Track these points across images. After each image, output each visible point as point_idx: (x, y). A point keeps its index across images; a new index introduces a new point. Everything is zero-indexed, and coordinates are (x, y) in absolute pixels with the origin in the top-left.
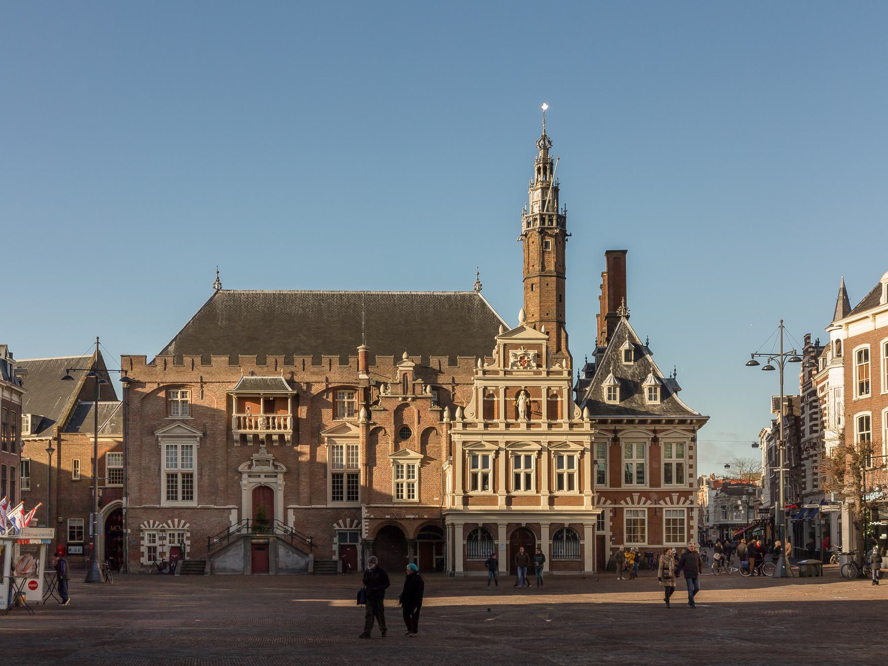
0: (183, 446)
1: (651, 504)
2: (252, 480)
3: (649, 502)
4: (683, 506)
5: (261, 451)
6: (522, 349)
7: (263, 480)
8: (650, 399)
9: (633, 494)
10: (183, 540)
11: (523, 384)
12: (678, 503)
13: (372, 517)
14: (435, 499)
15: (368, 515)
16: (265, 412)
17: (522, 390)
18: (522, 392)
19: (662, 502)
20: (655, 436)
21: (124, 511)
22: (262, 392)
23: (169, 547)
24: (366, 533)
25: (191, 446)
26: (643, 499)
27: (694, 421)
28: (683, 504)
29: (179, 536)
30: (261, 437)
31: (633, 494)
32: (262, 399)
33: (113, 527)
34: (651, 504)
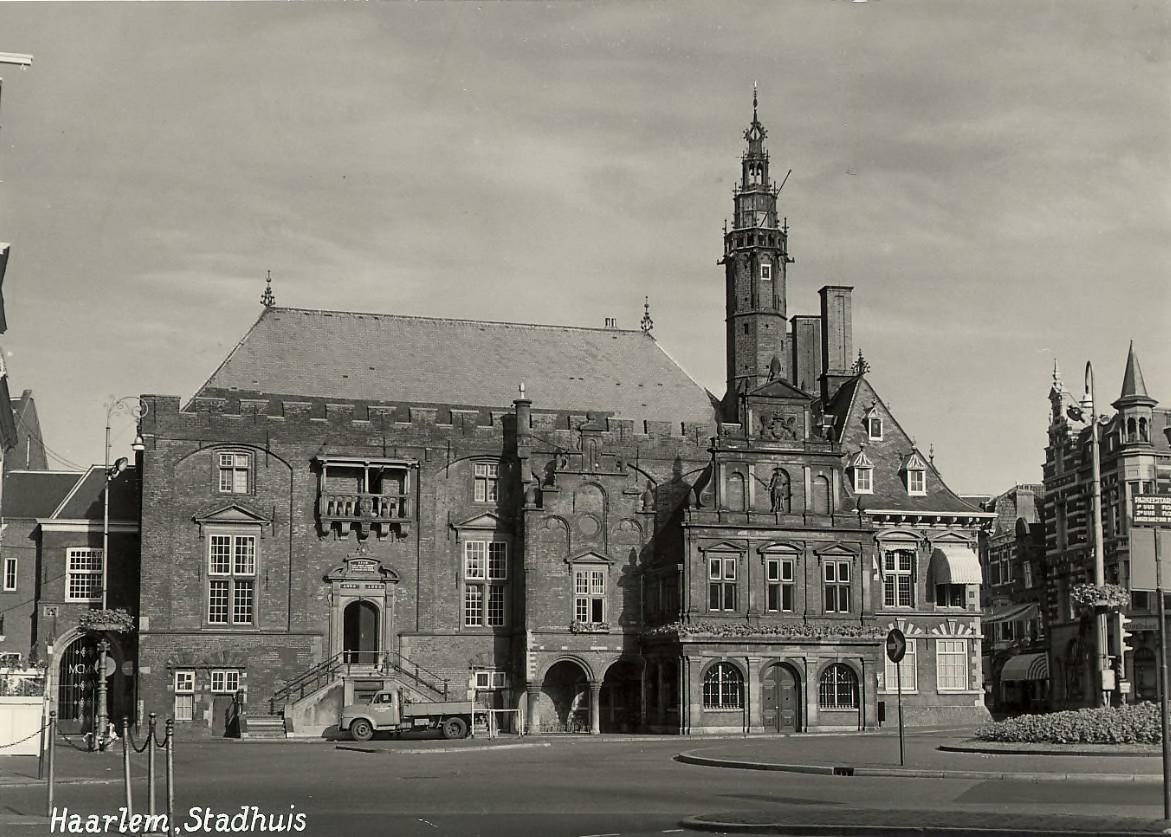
2: (342, 591)
3: (918, 630)
7: (363, 592)
8: (914, 489)
10: (235, 684)
13: (542, 648)
14: (632, 622)
15: (535, 645)
16: (370, 492)
19: (935, 631)
21: (142, 638)
22: (367, 460)
24: (532, 672)
26: (911, 626)
27: (978, 520)
28: (963, 633)
29: (229, 679)
32: (367, 472)
33: (73, 667)
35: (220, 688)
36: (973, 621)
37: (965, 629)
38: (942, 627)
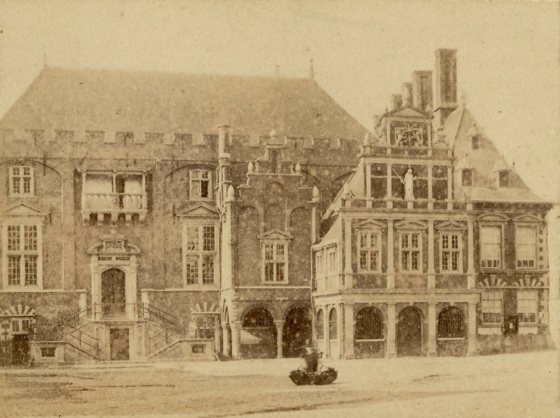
0: (25, 227)
1: (506, 285)
2: (101, 262)
3: (505, 283)
4: (535, 287)
5: (113, 232)
6: (409, 127)
7: (114, 262)
9: (491, 276)
11: (410, 162)
12: (530, 285)
17: (407, 169)
18: (410, 171)
20: (511, 220)
23: (13, 335)
25: (35, 228)
28: (535, 285)
30: (114, 218)
31: (491, 276)
34: (506, 285)
35: (18, 330)
36: (542, 276)
37: (537, 282)
38: (521, 280)
